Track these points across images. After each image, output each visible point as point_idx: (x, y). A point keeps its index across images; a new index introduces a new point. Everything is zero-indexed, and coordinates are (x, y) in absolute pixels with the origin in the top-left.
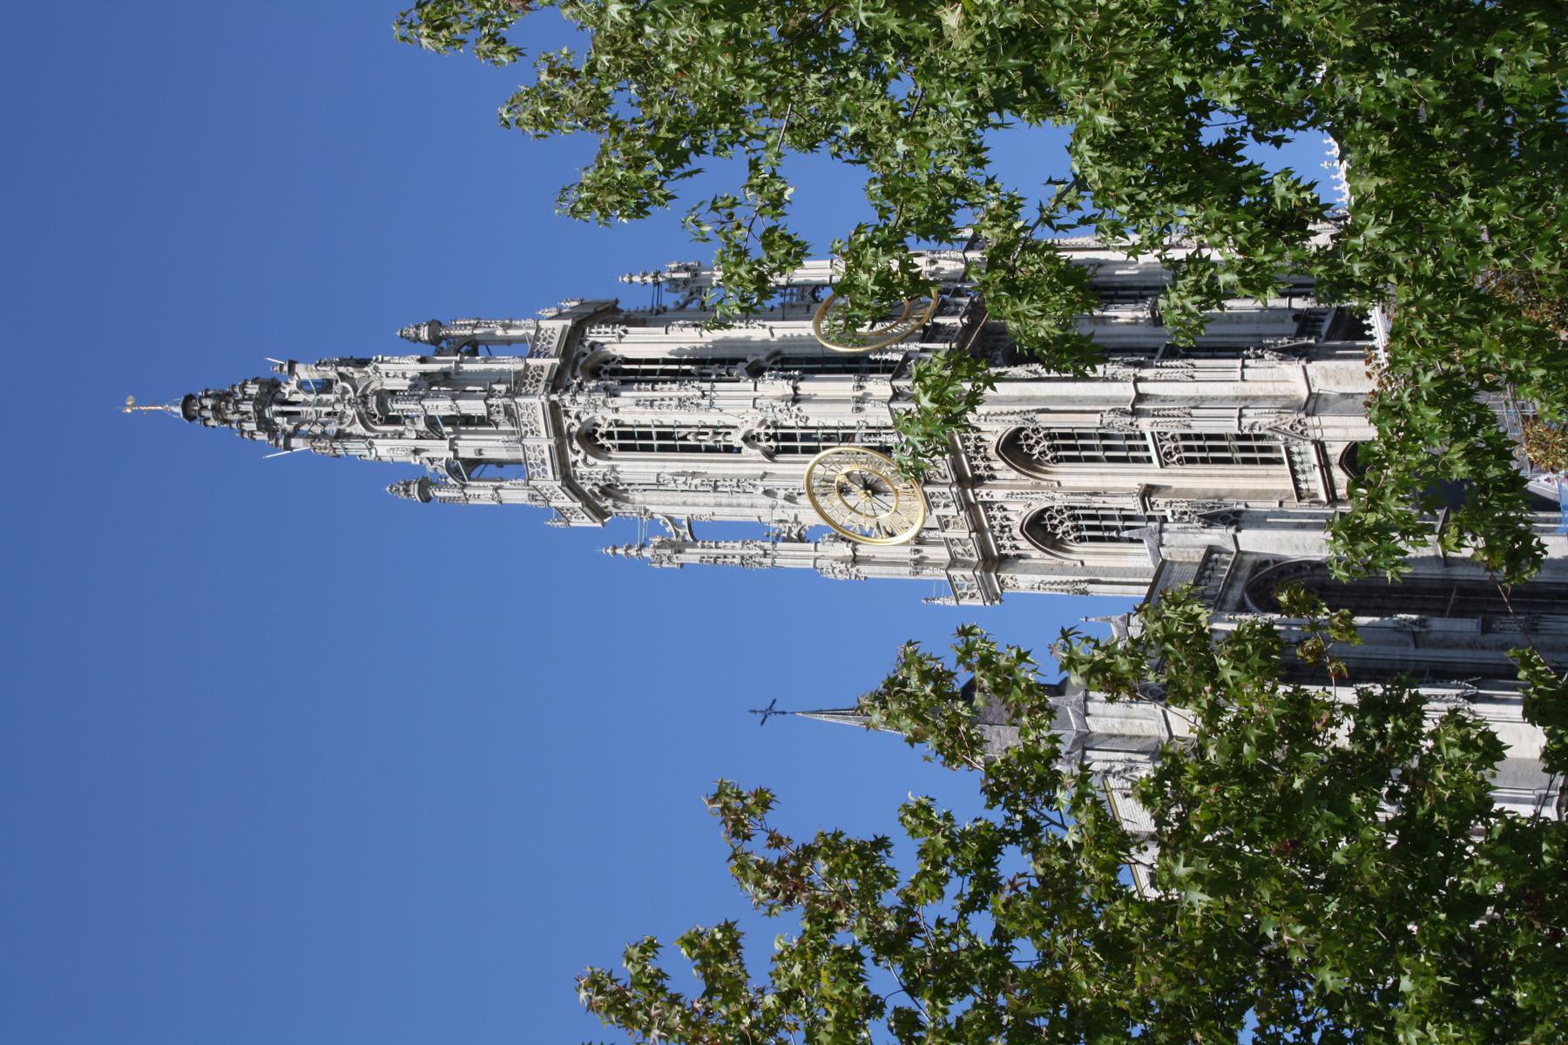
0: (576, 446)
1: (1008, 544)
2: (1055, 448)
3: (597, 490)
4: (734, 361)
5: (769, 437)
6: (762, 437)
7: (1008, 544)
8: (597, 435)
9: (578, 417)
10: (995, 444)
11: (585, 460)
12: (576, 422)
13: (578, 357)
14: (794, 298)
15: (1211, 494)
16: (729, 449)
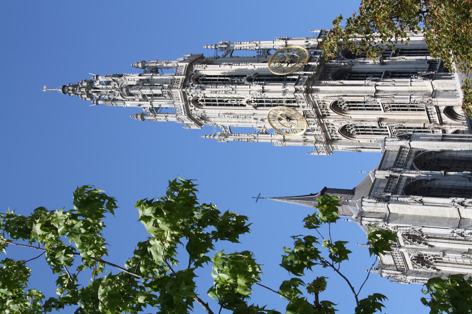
0: (192, 104)
1: (334, 135)
2: (350, 106)
3: (199, 118)
4: (242, 76)
5: (255, 102)
6: (252, 101)
7: (334, 135)
8: (198, 101)
9: (192, 95)
10: (329, 105)
11: (195, 109)
12: (191, 97)
13: (191, 75)
14: (262, 53)
15: (401, 121)
16: (242, 105)
